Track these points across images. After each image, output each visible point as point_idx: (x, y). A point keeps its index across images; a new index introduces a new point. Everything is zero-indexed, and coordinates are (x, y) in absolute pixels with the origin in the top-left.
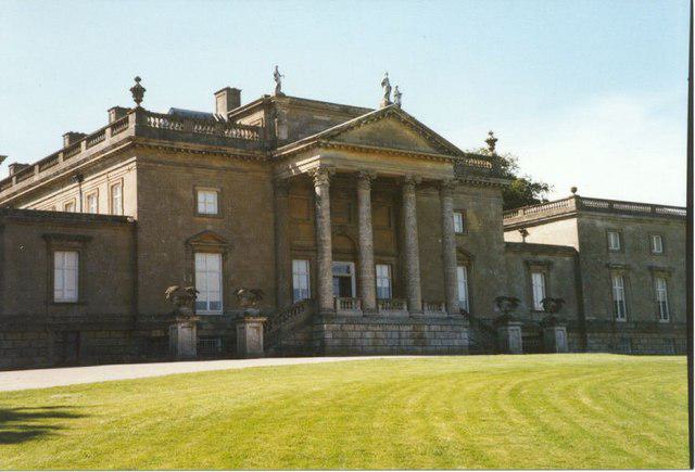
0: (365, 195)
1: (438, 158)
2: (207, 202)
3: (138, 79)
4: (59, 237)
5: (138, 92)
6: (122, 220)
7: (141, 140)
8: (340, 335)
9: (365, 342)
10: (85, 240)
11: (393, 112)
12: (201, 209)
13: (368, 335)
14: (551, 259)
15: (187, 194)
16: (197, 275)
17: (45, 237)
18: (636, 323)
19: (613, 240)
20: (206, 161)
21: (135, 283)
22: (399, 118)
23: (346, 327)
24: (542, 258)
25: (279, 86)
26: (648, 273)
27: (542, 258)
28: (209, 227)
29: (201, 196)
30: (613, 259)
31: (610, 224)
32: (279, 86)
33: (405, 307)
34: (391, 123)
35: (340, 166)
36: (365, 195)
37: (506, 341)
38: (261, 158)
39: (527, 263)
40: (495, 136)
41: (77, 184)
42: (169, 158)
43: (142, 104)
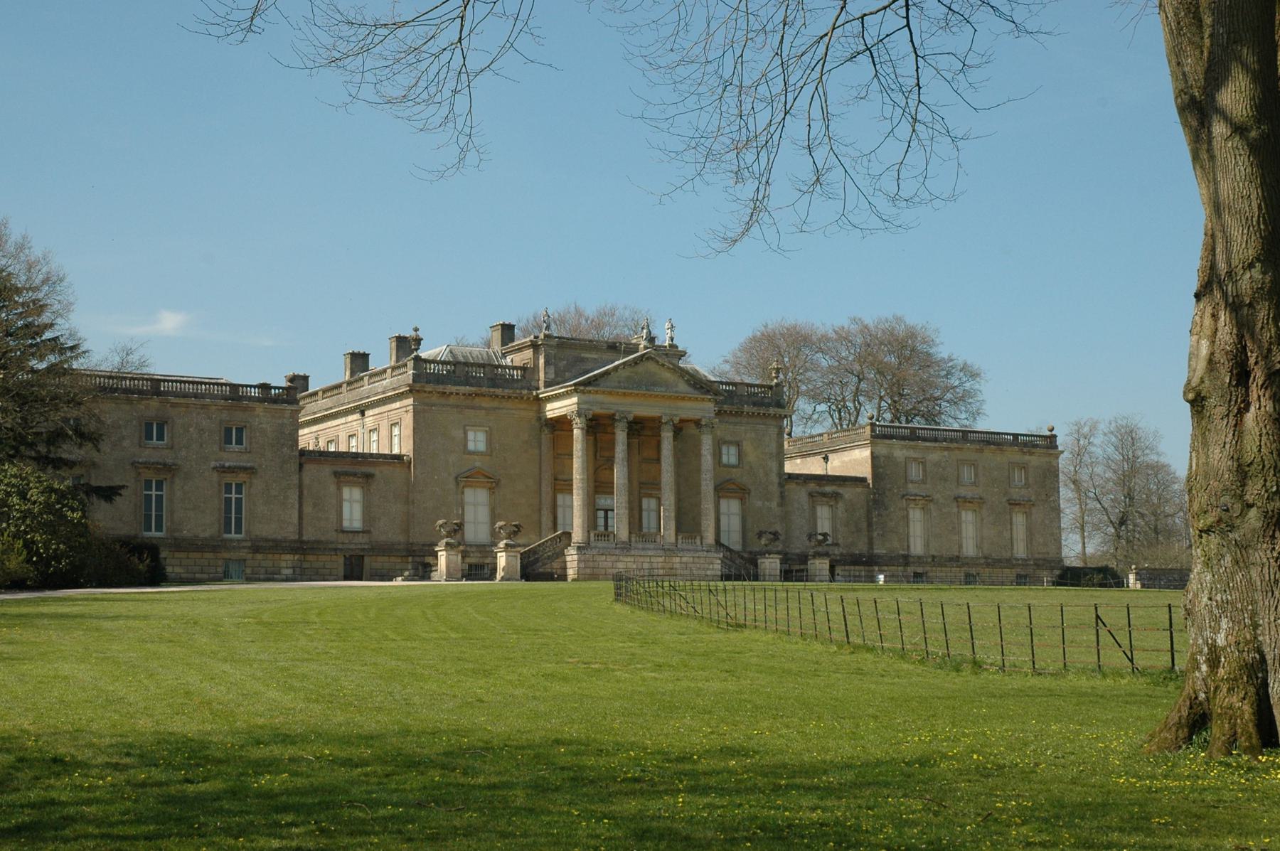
0: (621, 436)
2: (476, 441)
4: (346, 474)
6: (399, 457)
7: (418, 386)
8: (591, 564)
10: (368, 476)
12: (471, 446)
14: (841, 490)
15: (458, 433)
16: (466, 508)
17: (336, 474)
18: (934, 557)
19: (915, 472)
20: (477, 401)
23: (597, 558)
24: (828, 489)
26: (955, 504)
27: (828, 489)
28: (478, 464)
29: (471, 435)
30: (912, 488)
31: (912, 454)
35: (598, 410)
39: (811, 495)
42: (443, 401)
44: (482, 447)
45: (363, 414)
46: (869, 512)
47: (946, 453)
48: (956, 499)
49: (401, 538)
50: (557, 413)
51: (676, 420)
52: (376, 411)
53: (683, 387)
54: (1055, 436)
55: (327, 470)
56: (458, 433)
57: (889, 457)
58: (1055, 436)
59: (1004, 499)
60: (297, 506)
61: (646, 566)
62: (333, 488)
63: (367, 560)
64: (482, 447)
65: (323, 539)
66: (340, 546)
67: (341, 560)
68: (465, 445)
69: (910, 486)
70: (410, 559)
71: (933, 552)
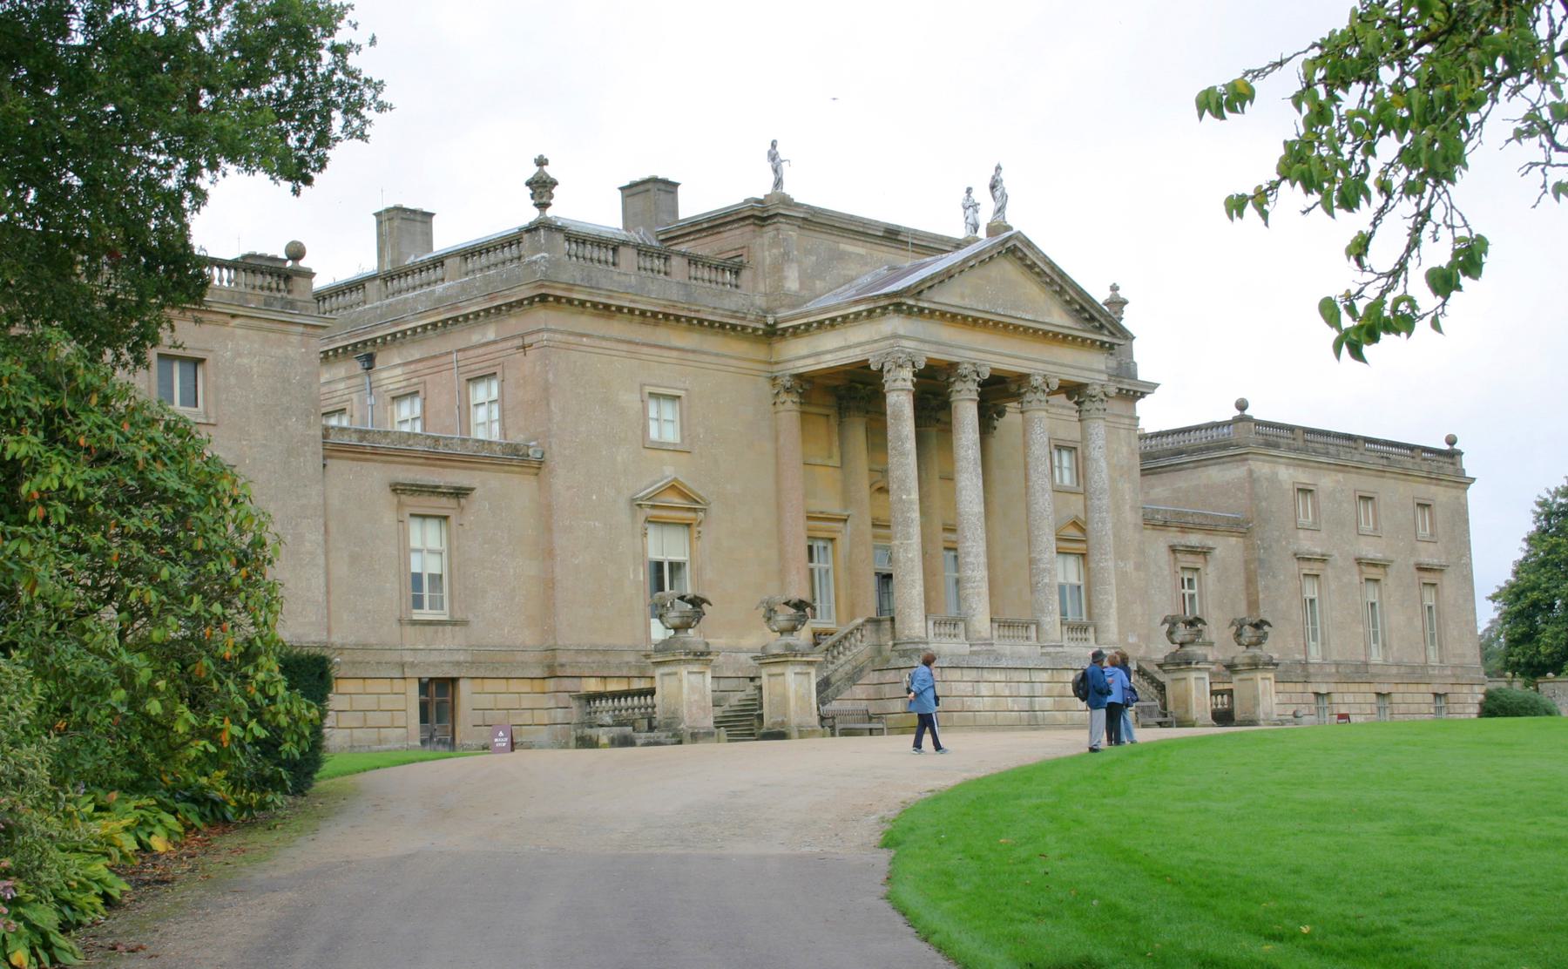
0: (966, 412)
1: (1084, 340)
2: (665, 426)
3: (541, 162)
5: (542, 187)
9: (977, 704)
10: (459, 493)
11: (1015, 250)
12: (654, 434)
13: (985, 689)
14: (1209, 541)
17: (397, 489)
18: (1338, 664)
21: (549, 584)
22: (1023, 258)
25: (778, 183)
27: (1194, 539)
30: (1307, 544)
32: (778, 183)
33: (1034, 635)
34: (1008, 270)
36: (966, 412)
37: (1185, 702)
38: (755, 330)
39: (1173, 549)
40: (1122, 294)
41: (357, 367)
43: (550, 212)
44: (671, 434)
45: (369, 360)
46: (1250, 581)
47: (1340, 476)
48: (1359, 562)
49: (527, 637)
50: (830, 361)
51: (1055, 385)
52: (415, 352)
53: (1058, 318)
54: (1460, 453)
55: (377, 476)
56: (629, 399)
57: (1273, 480)
58: (1460, 453)
59: (1412, 561)
60: (321, 561)
61: (1024, 689)
62: (389, 518)
63: (464, 688)
64: (671, 434)
65: (373, 640)
66: (408, 658)
67: (413, 689)
68: (645, 430)
69: (1301, 534)
70: (551, 684)
71: (1336, 657)
